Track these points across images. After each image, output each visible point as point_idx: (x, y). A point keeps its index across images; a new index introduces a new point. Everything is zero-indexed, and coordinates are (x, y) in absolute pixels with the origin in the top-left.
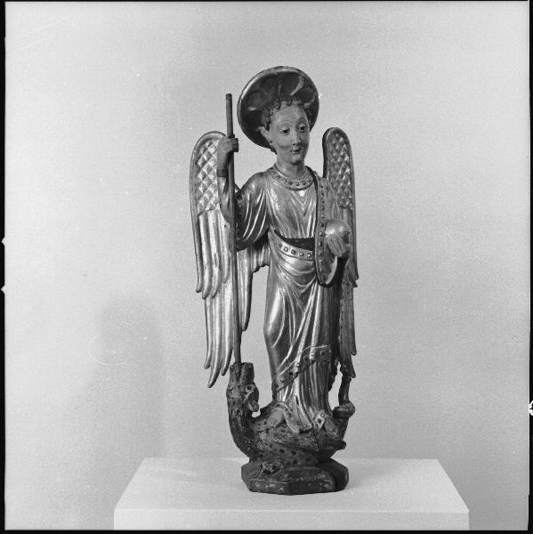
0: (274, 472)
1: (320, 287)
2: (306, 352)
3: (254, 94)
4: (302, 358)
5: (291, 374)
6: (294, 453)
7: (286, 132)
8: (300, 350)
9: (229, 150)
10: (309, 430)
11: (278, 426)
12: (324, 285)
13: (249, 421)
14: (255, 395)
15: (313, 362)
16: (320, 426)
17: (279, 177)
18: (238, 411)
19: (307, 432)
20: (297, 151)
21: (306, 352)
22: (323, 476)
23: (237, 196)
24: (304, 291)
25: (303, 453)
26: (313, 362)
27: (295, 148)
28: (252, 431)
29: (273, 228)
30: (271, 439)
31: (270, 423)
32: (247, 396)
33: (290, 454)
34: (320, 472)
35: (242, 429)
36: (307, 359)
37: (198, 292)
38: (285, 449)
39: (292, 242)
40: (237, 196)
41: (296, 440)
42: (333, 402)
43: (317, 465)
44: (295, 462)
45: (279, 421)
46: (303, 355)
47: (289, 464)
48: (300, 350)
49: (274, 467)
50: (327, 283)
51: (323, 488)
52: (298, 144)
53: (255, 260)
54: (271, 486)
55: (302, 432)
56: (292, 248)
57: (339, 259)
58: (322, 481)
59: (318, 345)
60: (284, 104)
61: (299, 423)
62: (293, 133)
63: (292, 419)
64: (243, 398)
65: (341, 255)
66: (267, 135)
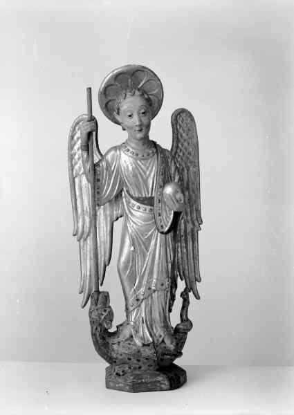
0: (123, 375)
1: (159, 234)
2: (149, 282)
3: (109, 88)
5: (138, 300)
6: (138, 360)
7: (130, 116)
8: (144, 282)
9: (89, 130)
11: (127, 340)
12: (162, 233)
13: (106, 336)
14: (111, 314)
15: (155, 291)
16: (161, 339)
17: (128, 150)
18: (96, 329)
19: (148, 345)
20: (141, 130)
21: (149, 282)
22: (160, 378)
23: (95, 167)
25: (146, 361)
26: (155, 291)
27: (138, 128)
29: (125, 189)
30: (121, 350)
31: (121, 338)
32: (103, 317)
33: (136, 362)
34: (159, 375)
35: (100, 341)
36: (150, 289)
37: (75, 235)
38: (132, 357)
39: (138, 200)
40: (95, 167)
41: (139, 352)
43: (157, 370)
44: (140, 368)
45: (128, 336)
47: (135, 369)
48: (144, 282)
49: (123, 371)
50: (166, 229)
52: (140, 125)
53: (115, 212)
54: (120, 385)
55: (144, 345)
57: (175, 213)
58: (159, 382)
60: (129, 94)
61: (143, 338)
64: (100, 318)
65: (175, 210)
66: (118, 118)
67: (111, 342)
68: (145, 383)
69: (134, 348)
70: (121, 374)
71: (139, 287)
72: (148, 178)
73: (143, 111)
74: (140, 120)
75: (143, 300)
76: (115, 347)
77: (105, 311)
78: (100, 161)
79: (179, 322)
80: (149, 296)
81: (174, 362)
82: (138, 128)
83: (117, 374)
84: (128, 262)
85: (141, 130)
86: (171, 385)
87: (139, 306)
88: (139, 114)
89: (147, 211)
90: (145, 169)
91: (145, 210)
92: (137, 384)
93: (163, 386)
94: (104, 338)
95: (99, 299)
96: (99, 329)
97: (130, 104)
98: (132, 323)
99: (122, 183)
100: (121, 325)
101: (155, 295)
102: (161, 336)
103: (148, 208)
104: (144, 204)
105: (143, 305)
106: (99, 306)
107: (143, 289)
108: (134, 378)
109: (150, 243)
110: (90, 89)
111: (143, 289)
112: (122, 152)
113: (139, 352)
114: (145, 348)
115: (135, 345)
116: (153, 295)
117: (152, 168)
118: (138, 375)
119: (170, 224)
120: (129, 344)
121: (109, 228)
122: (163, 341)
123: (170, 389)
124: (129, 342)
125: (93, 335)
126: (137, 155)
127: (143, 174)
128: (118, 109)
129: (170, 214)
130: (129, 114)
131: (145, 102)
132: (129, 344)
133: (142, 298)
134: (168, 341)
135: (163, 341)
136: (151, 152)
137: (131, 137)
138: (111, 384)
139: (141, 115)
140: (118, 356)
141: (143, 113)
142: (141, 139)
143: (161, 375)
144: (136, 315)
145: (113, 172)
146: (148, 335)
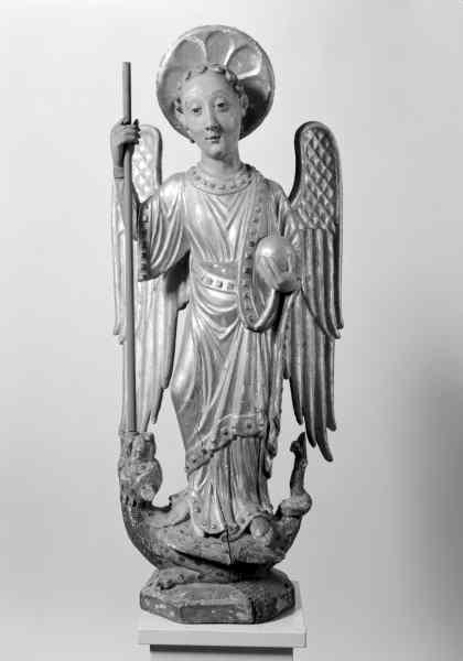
0: (170, 588)
1: (247, 331)
5: (205, 452)
7: (196, 110)
8: (217, 421)
10: (220, 534)
12: (251, 329)
14: (155, 480)
16: (243, 527)
17: (199, 178)
19: (217, 536)
23: (140, 208)
24: (222, 337)
27: (211, 134)
28: (148, 527)
32: (138, 480)
35: (134, 522)
36: (226, 434)
42: (278, 490)
45: (182, 516)
46: (220, 426)
48: (217, 421)
50: (257, 326)
51: (235, 617)
52: (213, 129)
54: (162, 606)
56: (215, 278)
57: (277, 292)
58: (232, 607)
62: (206, 110)
63: (200, 515)
64: (133, 481)
69: (189, 539)
70: (166, 586)
71: (204, 430)
72: (228, 228)
73: (219, 101)
74: (215, 120)
75: (214, 451)
76: (159, 535)
77: (144, 468)
78: (150, 198)
79: (288, 496)
80: (225, 446)
81: (276, 567)
82: (211, 134)
83: (159, 584)
84: (189, 378)
85: (216, 139)
86: (254, 613)
87: (207, 462)
88: (212, 106)
89: (224, 288)
90: (225, 210)
91: (221, 285)
92: (189, 607)
93: (239, 615)
94: (140, 518)
96: (131, 501)
97: (198, 90)
98: (193, 494)
99: (186, 238)
100: (176, 496)
101: (235, 445)
102: (243, 521)
103: (226, 282)
104: (220, 275)
108: (186, 597)
109: (228, 349)
110: (129, 65)
111: (211, 435)
112: (188, 183)
113: (197, 547)
114: (211, 540)
115: (192, 534)
117: (238, 209)
118: (195, 589)
119: (266, 314)
120: (182, 532)
121: (170, 323)
122: (247, 531)
123: (253, 623)
124: (182, 527)
126: (213, 186)
127: (220, 217)
128: (179, 101)
129: (266, 296)
130: (195, 106)
131: (226, 85)
132: (182, 532)
133: (212, 447)
134: (256, 532)
135: (247, 531)
136: (238, 182)
137: (206, 154)
138: (148, 603)
139: (217, 108)
141: (221, 105)
142: (218, 157)
143: (241, 594)
144: (201, 482)
145: (171, 217)
146: (219, 518)
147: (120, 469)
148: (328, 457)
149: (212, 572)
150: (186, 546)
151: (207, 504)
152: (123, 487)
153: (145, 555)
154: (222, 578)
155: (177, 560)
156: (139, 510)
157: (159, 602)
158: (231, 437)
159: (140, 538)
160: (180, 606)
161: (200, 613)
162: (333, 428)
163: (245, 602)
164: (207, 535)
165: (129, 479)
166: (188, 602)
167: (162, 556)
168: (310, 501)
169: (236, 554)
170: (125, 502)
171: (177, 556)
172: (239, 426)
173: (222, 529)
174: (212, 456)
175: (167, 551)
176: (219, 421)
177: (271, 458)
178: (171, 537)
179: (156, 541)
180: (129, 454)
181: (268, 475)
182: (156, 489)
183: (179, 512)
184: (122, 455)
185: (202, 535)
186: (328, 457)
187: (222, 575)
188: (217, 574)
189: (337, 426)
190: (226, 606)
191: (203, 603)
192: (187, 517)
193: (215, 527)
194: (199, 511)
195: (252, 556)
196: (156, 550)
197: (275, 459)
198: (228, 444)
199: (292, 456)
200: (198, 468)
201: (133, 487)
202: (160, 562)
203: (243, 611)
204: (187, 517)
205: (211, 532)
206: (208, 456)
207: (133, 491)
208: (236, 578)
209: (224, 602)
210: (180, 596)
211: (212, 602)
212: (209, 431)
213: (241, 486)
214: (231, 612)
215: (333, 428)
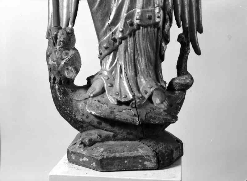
2: (130, 16)
4: (125, 23)
5: (115, 40)
8: (124, 14)
14: (75, 63)
15: (138, 28)
16: (146, 96)
19: (127, 103)
21: (130, 16)
26: (139, 26)
28: (71, 100)
32: (63, 63)
36: (132, 24)
42: (169, 71)
46: (127, 18)
48: (124, 14)
51: (143, 165)
54: (85, 159)
55: (120, 103)
58: (141, 157)
59: (143, 8)
64: (59, 64)
67: (75, 98)
68: (120, 158)
70: (87, 144)
76: (81, 105)
77: (67, 54)
79: (175, 75)
80: (130, 35)
83: (82, 143)
86: (158, 162)
92: (108, 158)
93: (146, 163)
94: (65, 94)
95: (63, 40)
96: (58, 79)
101: (140, 33)
102: (146, 93)
105: (121, 48)
106: (58, 47)
107: (120, 26)
111: (120, 26)
114: (124, 107)
115: (107, 103)
116: (137, 32)
118: (109, 145)
120: (99, 101)
123: (158, 169)
124: (99, 98)
125: (52, 88)
132: (99, 101)
134: (157, 100)
135: (150, 100)
140: (84, 118)
143: (146, 147)
147: (48, 56)
148: (198, 52)
149: (122, 133)
150: (104, 111)
151: (117, 81)
152: (50, 70)
153: (70, 122)
154: (131, 136)
155: (95, 124)
156: (63, 88)
157: (83, 156)
158: (135, 27)
159: (65, 108)
160: (99, 158)
161: (116, 163)
162: (201, 31)
163: (151, 154)
164: (120, 103)
165: (55, 63)
166: (106, 155)
167: (83, 122)
168: (192, 79)
169: (143, 116)
170: (53, 81)
171: (96, 120)
172: (140, 19)
173: (130, 96)
174: (120, 43)
175: (87, 117)
176: (125, 15)
177: (166, 44)
178: (90, 106)
179: (78, 110)
180: (55, 44)
181: (162, 59)
182: (77, 71)
183: (96, 86)
184: (49, 45)
185: (116, 103)
186: (198, 52)
187: (131, 134)
188: (128, 133)
189: (204, 30)
190: (135, 157)
191: (118, 155)
192: (103, 91)
193: (126, 97)
194: (112, 85)
195: (154, 119)
196: (79, 118)
197: (168, 45)
198: (133, 34)
199: (178, 46)
200: (109, 54)
201: (59, 69)
202: (82, 127)
203: (148, 160)
204: (103, 91)
205: (123, 100)
206: (117, 43)
207: (59, 72)
208: (142, 136)
209: (135, 154)
210: (99, 151)
211: (126, 154)
212: (117, 23)
213: (143, 66)
214: (140, 161)
215: (201, 31)
